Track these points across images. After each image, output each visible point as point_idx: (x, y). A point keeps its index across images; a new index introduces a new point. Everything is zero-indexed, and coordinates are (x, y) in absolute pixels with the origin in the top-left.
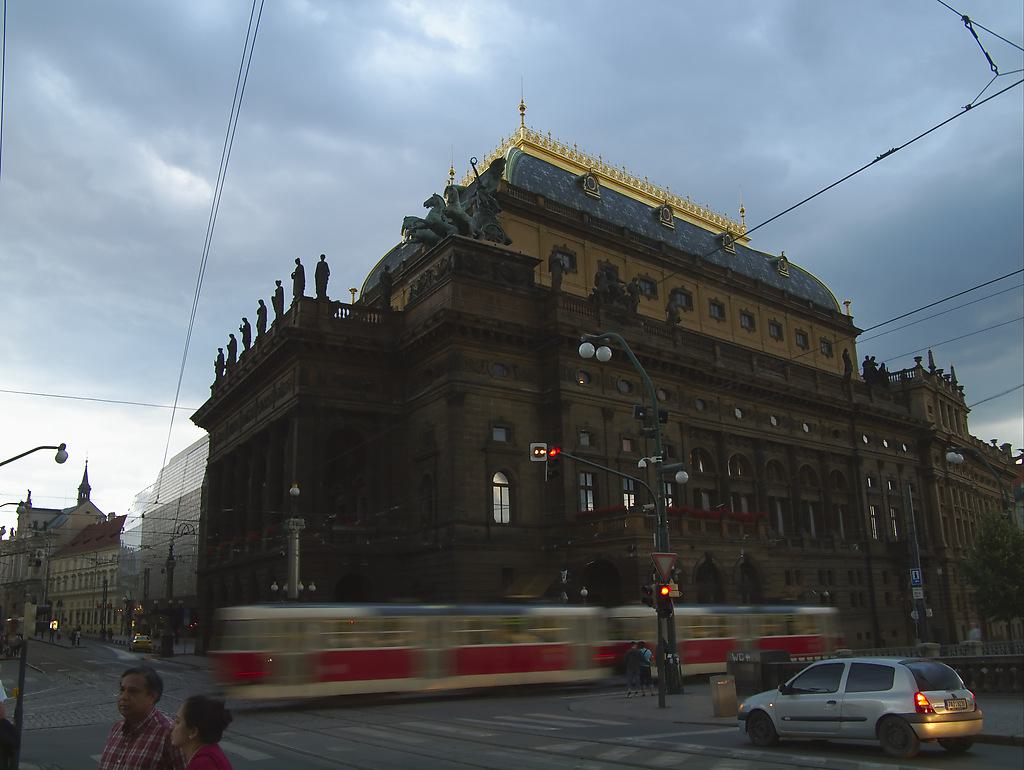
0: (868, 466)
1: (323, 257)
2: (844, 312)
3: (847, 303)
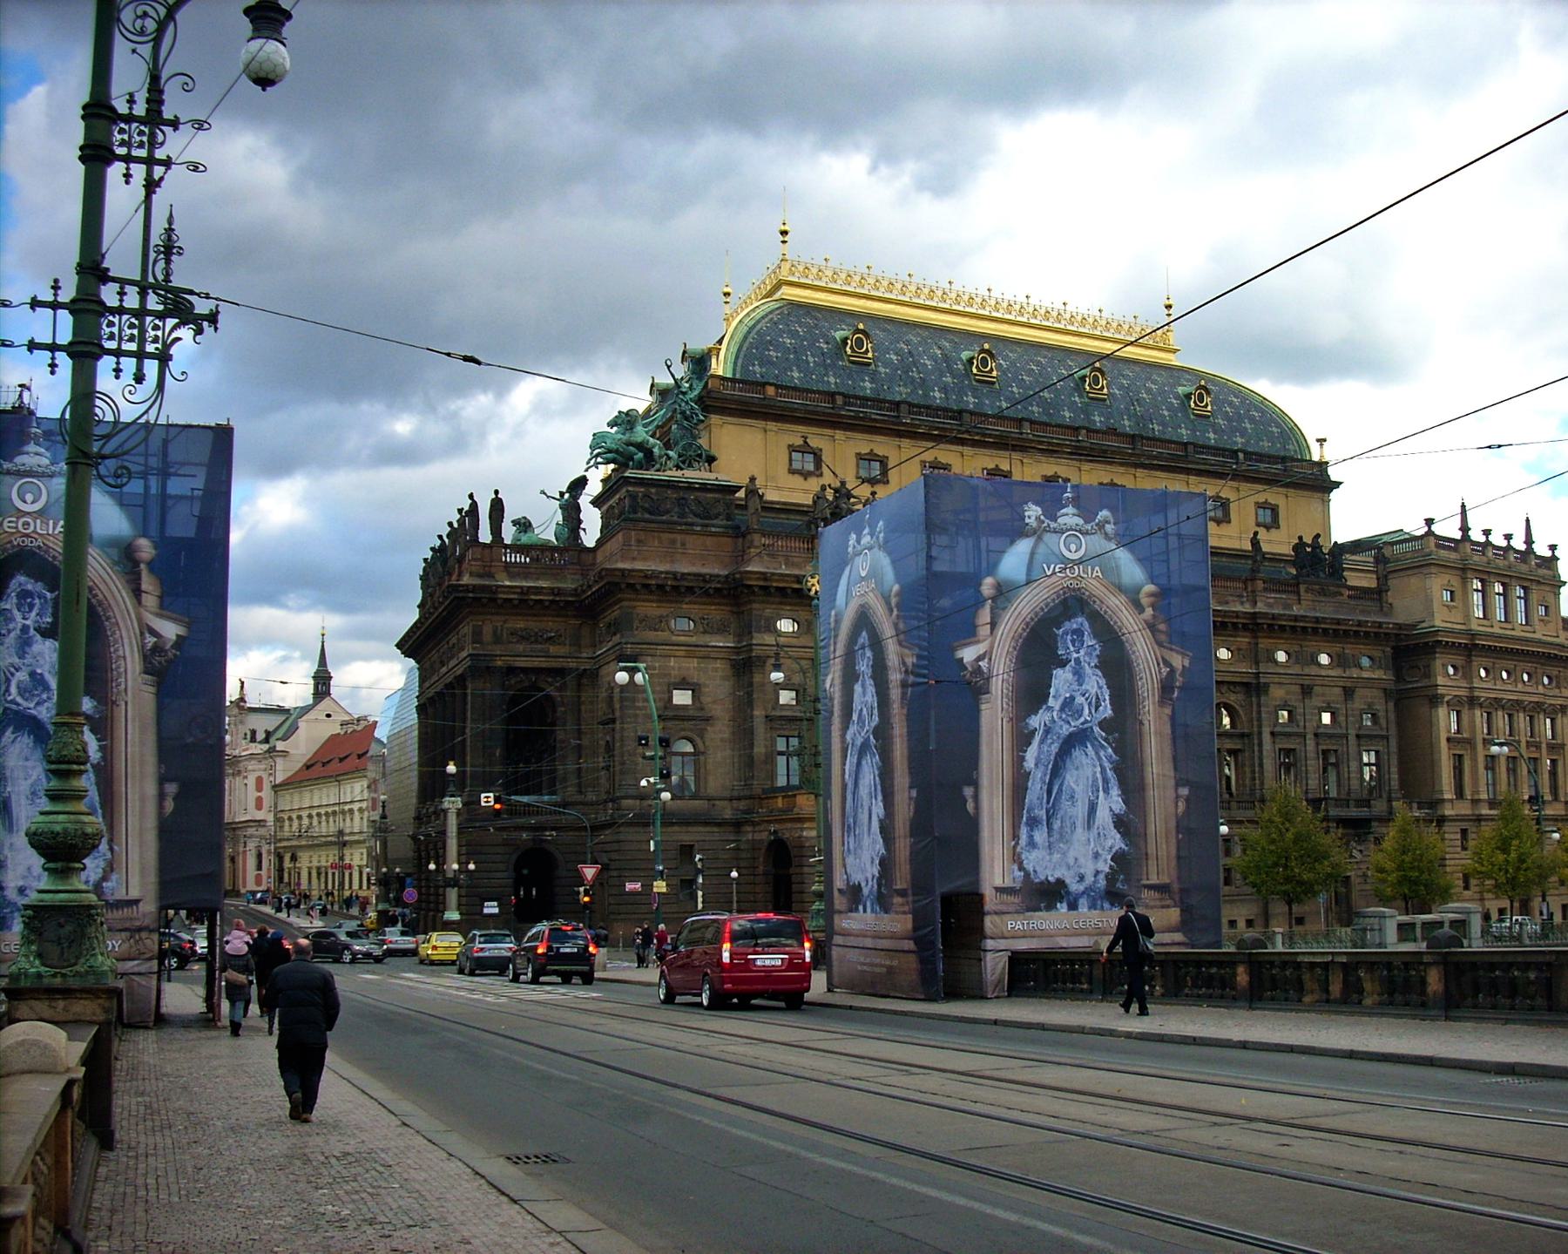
0: (1277, 693)
1: (496, 492)
2: (1316, 458)
3: (1321, 441)
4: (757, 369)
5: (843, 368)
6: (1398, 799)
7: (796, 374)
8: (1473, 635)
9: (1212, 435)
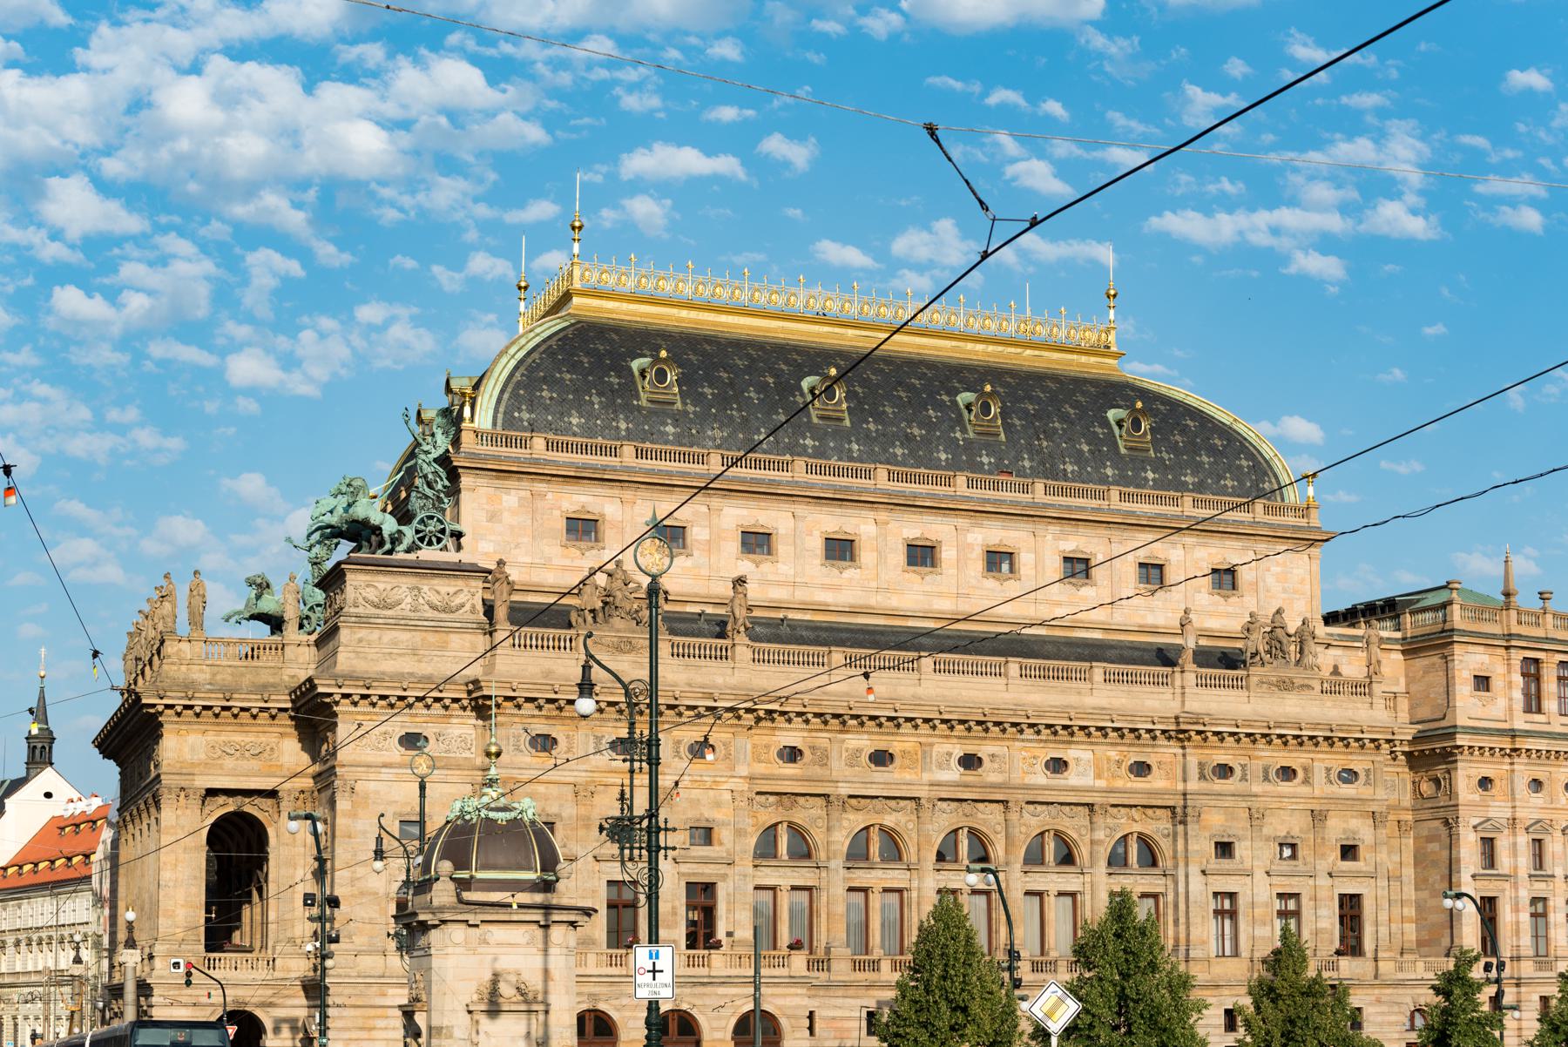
0: (1215, 822)
4: (526, 416)
5: (639, 408)
6: (1385, 959)
7: (575, 421)
8: (1513, 734)
9: (1150, 475)
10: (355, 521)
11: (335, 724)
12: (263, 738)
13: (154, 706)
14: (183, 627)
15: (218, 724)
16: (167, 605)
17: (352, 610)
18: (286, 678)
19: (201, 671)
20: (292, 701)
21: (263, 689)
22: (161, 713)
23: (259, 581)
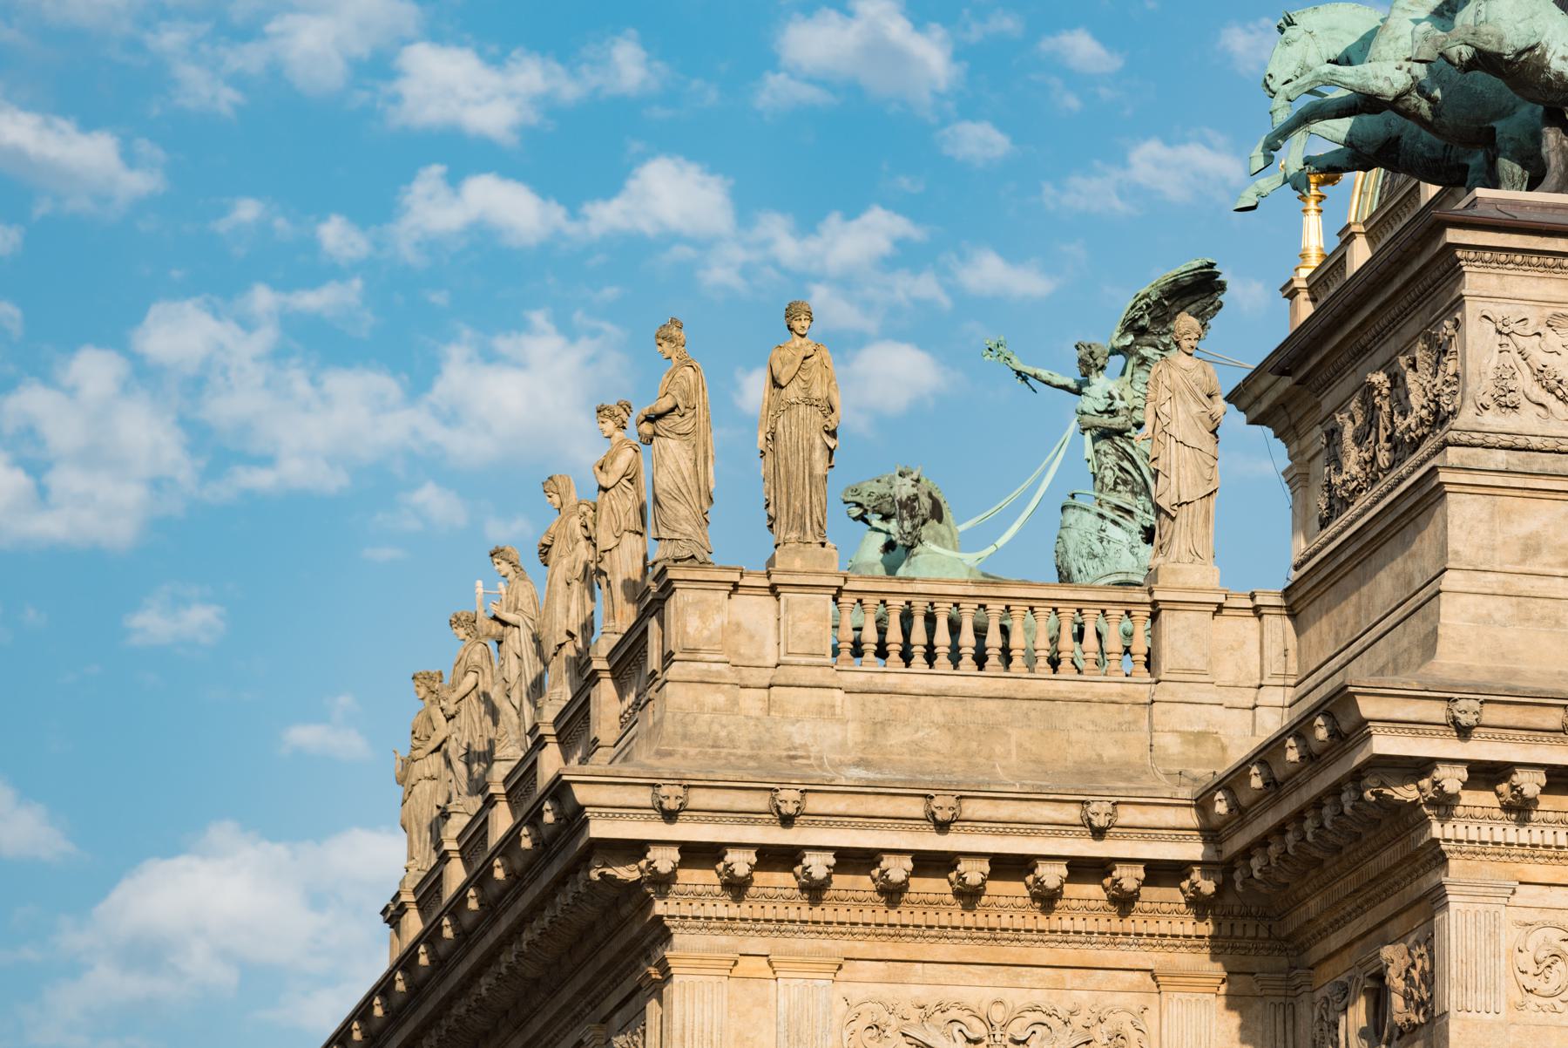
10: (1485, 61)
11: (1436, 899)
12: (1079, 994)
13: (635, 849)
14: (737, 538)
15: (897, 932)
16: (673, 453)
17: (1493, 420)
18: (1170, 744)
19: (826, 713)
20: (1211, 833)
21: (1088, 796)
22: (663, 883)
23: (904, 489)
